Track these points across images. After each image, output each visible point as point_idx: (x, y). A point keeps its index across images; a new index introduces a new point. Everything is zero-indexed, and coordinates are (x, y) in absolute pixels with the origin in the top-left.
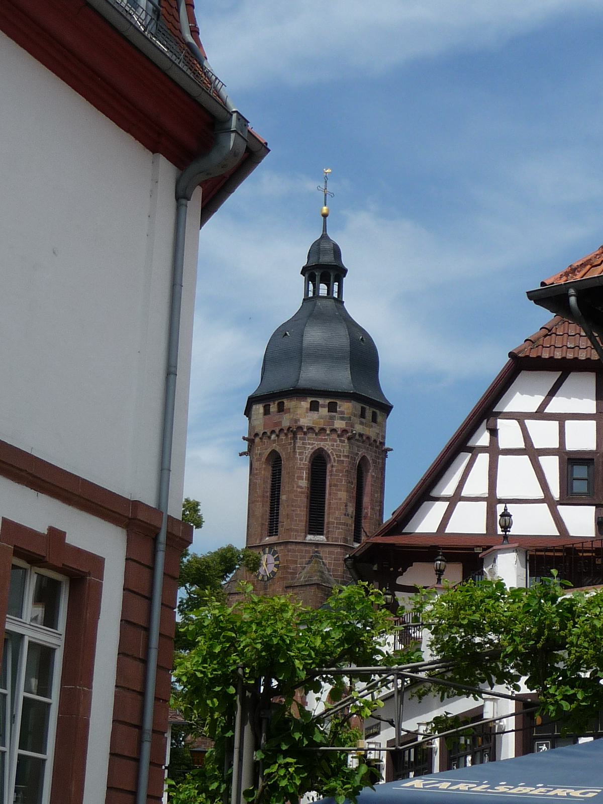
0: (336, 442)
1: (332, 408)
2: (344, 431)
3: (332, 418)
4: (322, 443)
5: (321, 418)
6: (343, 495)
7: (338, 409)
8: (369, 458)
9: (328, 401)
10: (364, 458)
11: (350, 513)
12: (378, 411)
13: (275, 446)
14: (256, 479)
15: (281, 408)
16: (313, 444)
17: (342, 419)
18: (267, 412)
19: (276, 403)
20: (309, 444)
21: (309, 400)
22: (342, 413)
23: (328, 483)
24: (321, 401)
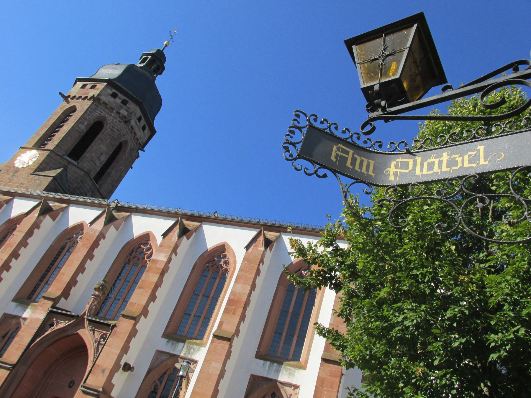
0: (116, 119)
1: (124, 102)
2: (125, 117)
3: (121, 107)
6: (103, 147)
8: (129, 144)
9: (124, 98)
10: (126, 142)
11: (102, 160)
12: (147, 128)
16: (101, 112)
17: (127, 111)
20: (99, 111)
21: (114, 90)
22: (129, 108)
23: (98, 137)
24: (120, 95)
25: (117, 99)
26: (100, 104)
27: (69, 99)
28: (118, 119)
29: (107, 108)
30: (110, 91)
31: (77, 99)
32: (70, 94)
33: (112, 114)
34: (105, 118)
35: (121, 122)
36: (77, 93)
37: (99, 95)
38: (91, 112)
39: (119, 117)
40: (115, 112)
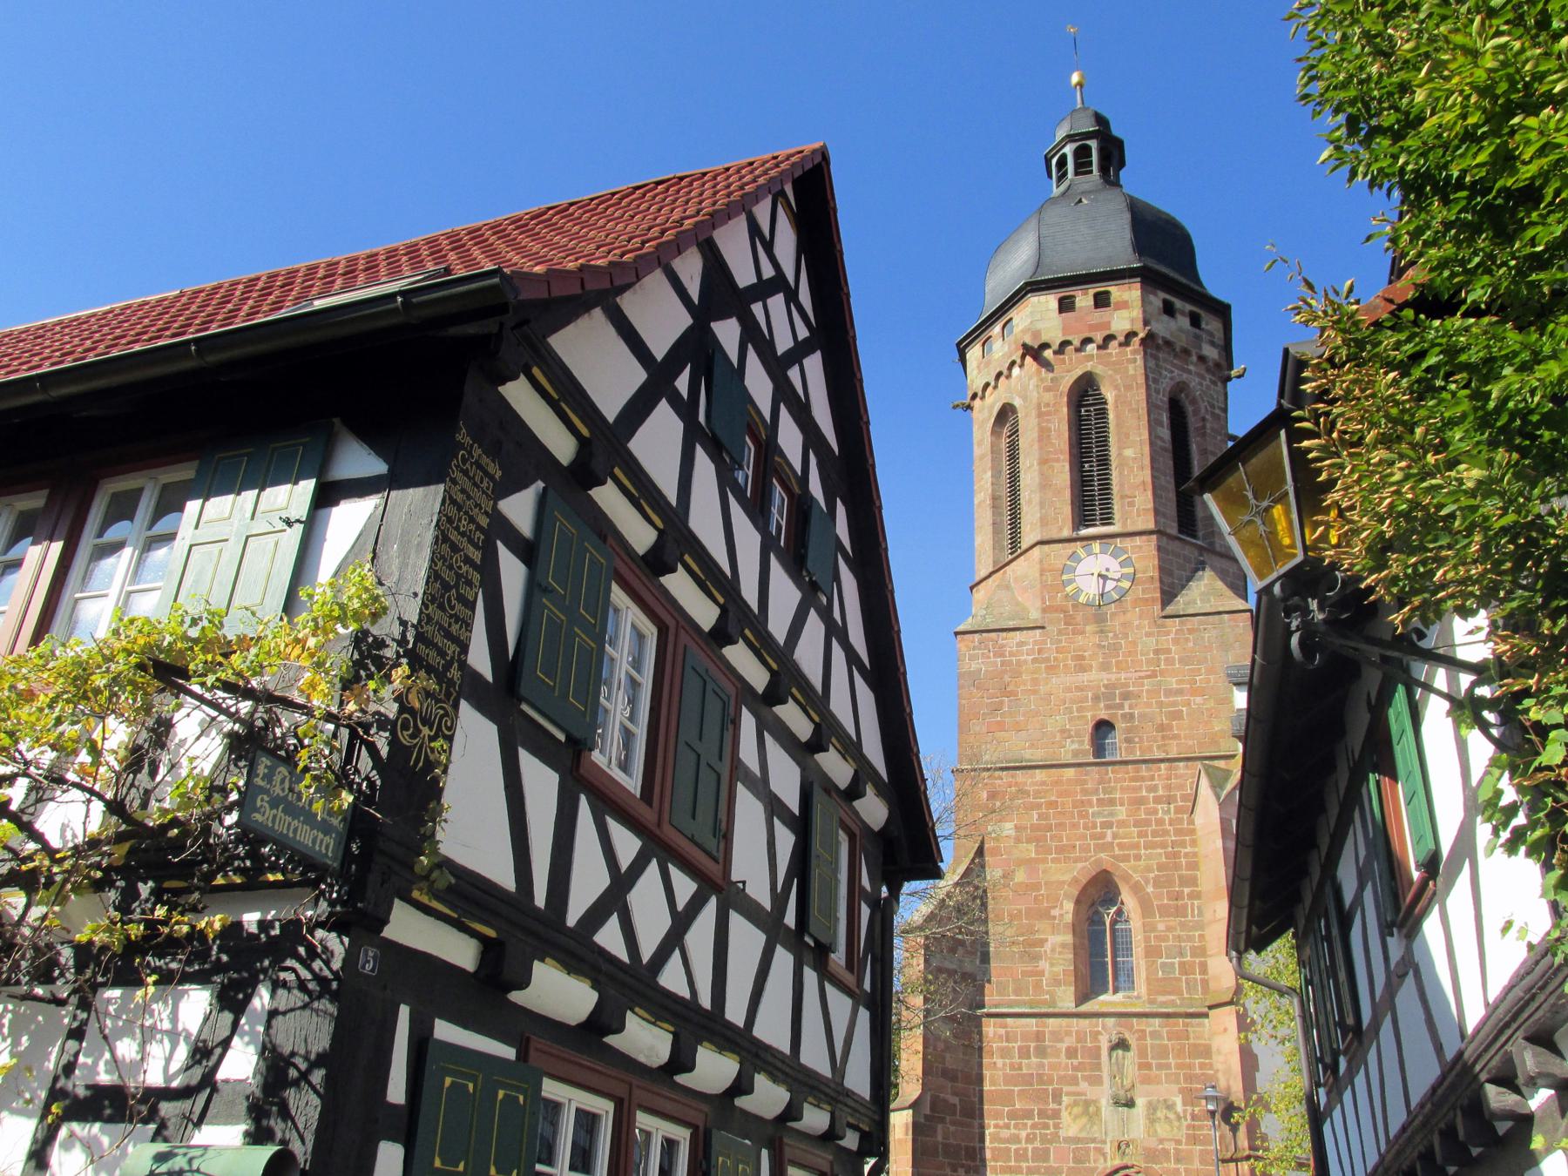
1: (1195, 321)
4: (1185, 376)
5: (1181, 330)
7: (1203, 325)
9: (1189, 307)
13: (1089, 367)
14: (1048, 421)
15: (1102, 301)
18: (1066, 305)
19: (1092, 292)
21: (1163, 295)
23: (1194, 447)
24: (1178, 304)
25: (1179, 317)
26: (1158, 348)
27: (1048, 354)
28: (1208, 376)
29: (1176, 356)
30: (1157, 300)
31: (1077, 350)
32: (1044, 338)
33: (1191, 367)
34: (1181, 387)
35: (1215, 383)
36: (1065, 330)
37: (1146, 323)
38: (1156, 381)
39: (1208, 370)
40: (1194, 358)
